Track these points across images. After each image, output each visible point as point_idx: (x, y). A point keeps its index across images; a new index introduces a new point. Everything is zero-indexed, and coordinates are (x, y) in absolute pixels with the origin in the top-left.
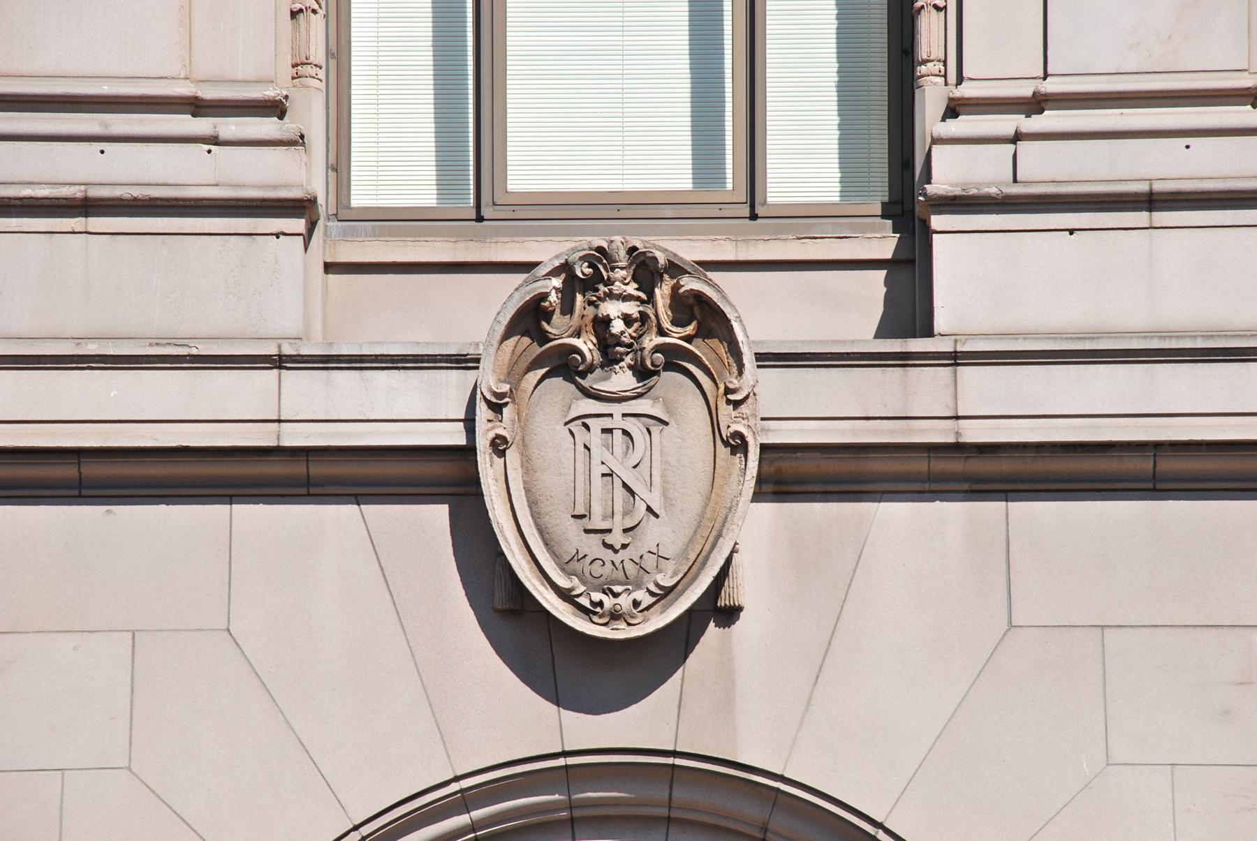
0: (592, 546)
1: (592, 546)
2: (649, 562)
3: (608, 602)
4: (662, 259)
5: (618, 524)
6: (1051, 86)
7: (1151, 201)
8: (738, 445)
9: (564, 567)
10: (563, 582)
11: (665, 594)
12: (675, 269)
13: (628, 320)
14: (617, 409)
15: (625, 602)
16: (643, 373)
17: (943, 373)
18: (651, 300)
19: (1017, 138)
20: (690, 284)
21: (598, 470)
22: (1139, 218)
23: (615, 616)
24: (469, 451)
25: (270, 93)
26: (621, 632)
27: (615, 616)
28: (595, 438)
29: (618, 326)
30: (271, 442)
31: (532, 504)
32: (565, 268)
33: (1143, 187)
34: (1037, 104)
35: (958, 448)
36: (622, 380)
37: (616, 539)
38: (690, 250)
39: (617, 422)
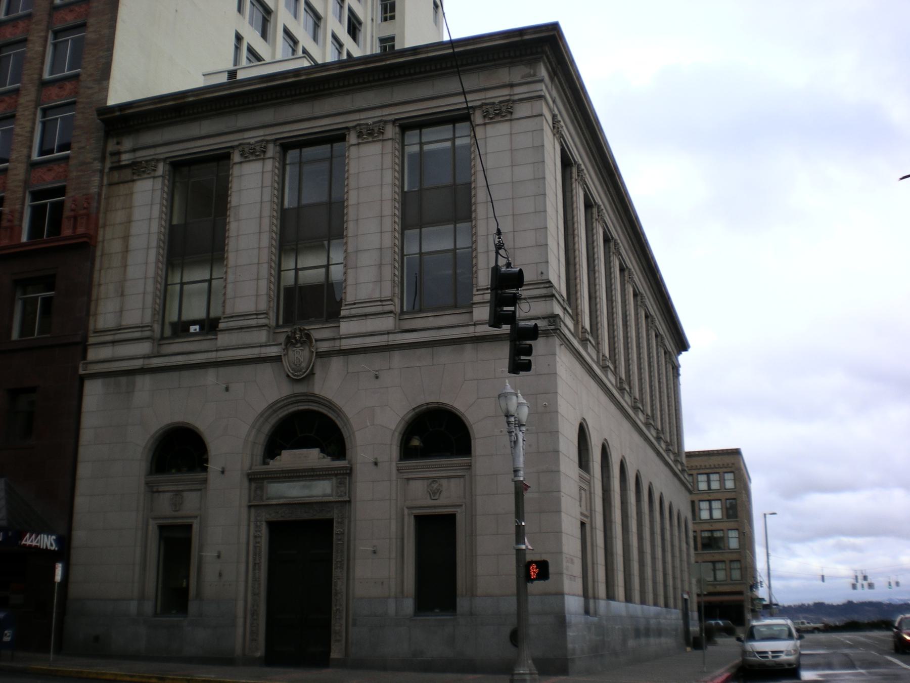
4: (302, 328)
8: (313, 352)
9: (292, 370)
10: (292, 372)
11: (305, 372)
12: (305, 329)
16: (301, 344)
17: (339, 340)
18: (301, 334)
20: (306, 332)
22: (364, 318)
25: (264, 312)
26: (298, 378)
27: (298, 376)
29: (298, 338)
30: (259, 357)
32: (291, 331)
36: (299, 345)
38: (307, 328)
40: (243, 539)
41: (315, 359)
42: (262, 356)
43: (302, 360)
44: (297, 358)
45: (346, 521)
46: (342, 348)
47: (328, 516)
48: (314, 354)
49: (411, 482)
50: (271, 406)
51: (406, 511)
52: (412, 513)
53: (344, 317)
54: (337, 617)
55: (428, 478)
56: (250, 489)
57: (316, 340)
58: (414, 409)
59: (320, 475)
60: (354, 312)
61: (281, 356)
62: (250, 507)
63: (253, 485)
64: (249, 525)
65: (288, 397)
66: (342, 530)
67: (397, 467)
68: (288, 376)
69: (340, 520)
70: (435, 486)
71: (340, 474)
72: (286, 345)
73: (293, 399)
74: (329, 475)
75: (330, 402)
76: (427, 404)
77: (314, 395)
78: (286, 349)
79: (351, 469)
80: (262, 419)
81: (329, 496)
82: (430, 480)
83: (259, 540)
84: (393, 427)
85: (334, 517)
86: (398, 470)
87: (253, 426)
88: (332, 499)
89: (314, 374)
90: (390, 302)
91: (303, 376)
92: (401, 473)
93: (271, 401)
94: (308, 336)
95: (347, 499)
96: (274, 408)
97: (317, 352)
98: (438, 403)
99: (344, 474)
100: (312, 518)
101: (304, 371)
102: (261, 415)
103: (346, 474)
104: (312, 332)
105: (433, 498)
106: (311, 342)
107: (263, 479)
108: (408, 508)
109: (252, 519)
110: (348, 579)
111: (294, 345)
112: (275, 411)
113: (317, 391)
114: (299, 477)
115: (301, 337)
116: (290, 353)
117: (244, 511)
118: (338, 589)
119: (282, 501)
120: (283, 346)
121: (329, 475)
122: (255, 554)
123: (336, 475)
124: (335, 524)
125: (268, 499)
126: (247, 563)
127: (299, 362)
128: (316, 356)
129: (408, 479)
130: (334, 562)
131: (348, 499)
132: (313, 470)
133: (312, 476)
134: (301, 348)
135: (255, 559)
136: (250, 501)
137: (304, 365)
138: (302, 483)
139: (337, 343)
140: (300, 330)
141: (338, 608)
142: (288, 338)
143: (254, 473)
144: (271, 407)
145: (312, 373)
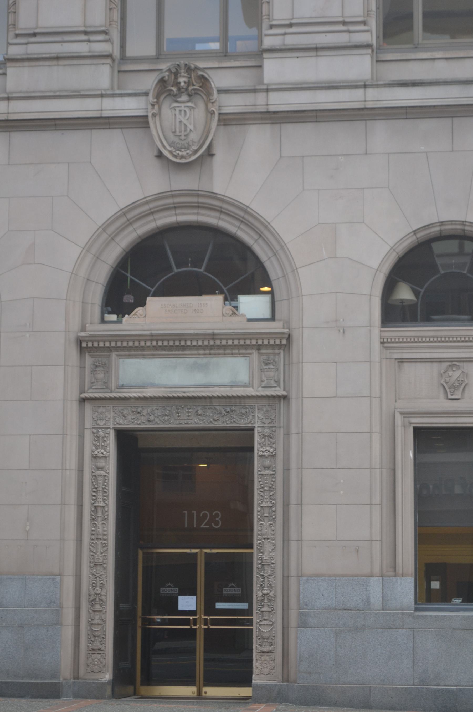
0: (176, 140)
1: (176, 140)
2: (191, 143)
3: (180, 153)
4: (193, 66)
5: (183, 133)
6: (294, 21)
7: (317, 49)
8: (213, 113)
9: (170, 146)
11: (196, 151)
12: (197, 68)
13: (185, 82)
14: (183, 105)
15: (184, 153)
16: (190, 96)
18: (190, 78)
19: (285, 34)
20: (200, 73)
21: (178, 120)
23: (182, 157)
24: (147, 117)
25: (103, 29)
26: (183, 161)
27: (182, 157)
28: (177, 112)
29: (182, 84)
31: (162, 130)
32: (169, 70)
33: (314, 46)
34: (291, 25)
35: (268, 112)
36: (184, 98)
37: (183, 137)
38: (201, 65)
39: (183, 108)
40: (72, 463)
41: (216, 130)
42: (106, 114)
43: (191, 127)
44: (180, 122)
45: (281, 434)
46: (272, 109)
47: (243, 423)
48: (216, 117)
49: (406, 365)
50: (124, 212)
51: (399, 419)
52: (411, 424)
53: (271, 50)
54: (266, 609)
55: (440, 361)
56: (82, 367)
57: (220, 91)
58: (415, 232)
59: (225, 347)
60: (291, 41)
61: (147, 117)
62: (83, 401)
63: (89, 360)
64: (81, 436)
65: (159, 197)
66: (271, 450)
67: (381, 337)
68: (160, 155)
69: (267, 431)
70: (455, 375)
71: (269, 346)
72: (158, 97)
73: (170, 201)
74: (246, 347)
75: (245, 210)
76: (442, 223)
77: (213, 196)
78: (157, 103)
79: (289, 338)
80: (105, 236)
82: (445, 365)
83: (101, 463)
84: (375, 264)
85: (256, 425)
86: (382, 343)
87: (87, 248)
88: (250, 391)
89: (212, 155)
90: (362, 27)
91: (193, 158)
92: (387, 348)
93: (124, 202)
94: (204, 81)
95: (280, 392)
96: (130, 216)
97: (220, 114)
98: (463, 223)
99: (274, 346)
101: (195, 148)
102: (105, 227)
103: (280, 346)
104: (209, 72)
105: (450, 397)
106: (209, 94)
107: (110, 349)
108: (402, 413)
109: (88, 424)
110: (286, 540)
111: (175, 97)
112: (130, 223)
113: (218, 188)
114: (184, 348)
115: (189, 83)
116: (166, 111)
117: (74, 407)
118: (265, 556)
119: (149, 393)
120: (151, 98)
122: (95, 490)
123: (259, 348)
124: (257, 438)
125: (122, 387)
126: (80, 506)
127: (185, 130)
128: (219, 120)
129: (401, 361)
130: (256, 508)
131: (285, 393)
132: (213, 336)
133: (211, 347)
134: (190, 104)
135: (94, 498)
136: (82, 392)
137: (194, 137)
138: (190, 361)
139: (261, 99)
140: (189, 69)
141: (265, 592)
142: (162, 81)
143: (93, 338)
144: (124, 214)
145: (210, 154)
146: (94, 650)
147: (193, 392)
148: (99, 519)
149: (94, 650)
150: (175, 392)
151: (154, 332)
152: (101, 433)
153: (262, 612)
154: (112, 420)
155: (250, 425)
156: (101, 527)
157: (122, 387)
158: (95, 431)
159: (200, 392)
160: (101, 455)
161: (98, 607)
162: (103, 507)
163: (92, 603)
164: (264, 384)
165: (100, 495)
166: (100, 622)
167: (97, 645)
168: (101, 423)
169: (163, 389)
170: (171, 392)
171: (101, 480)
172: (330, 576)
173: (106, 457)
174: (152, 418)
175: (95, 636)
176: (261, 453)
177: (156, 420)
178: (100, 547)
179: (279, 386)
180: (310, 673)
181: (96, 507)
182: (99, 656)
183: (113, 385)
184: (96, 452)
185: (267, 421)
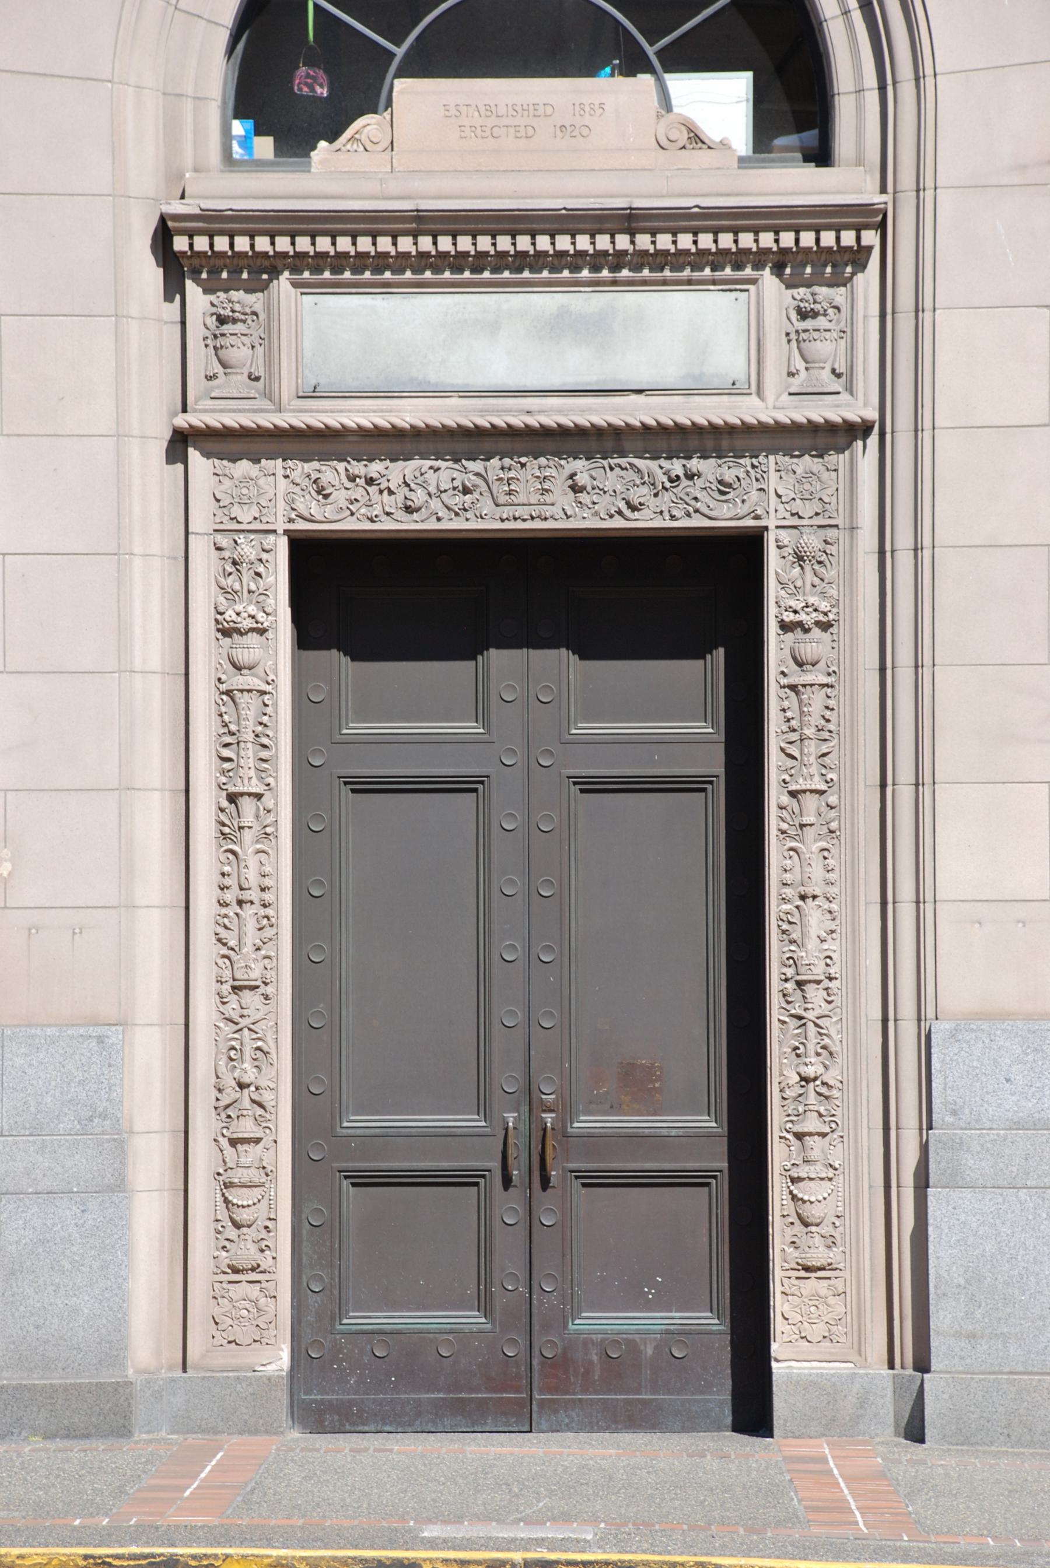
66: (824, 606)
74: (739, 259)
81: (733, 390)
83: (249, 649)
85: (771, 522)
100: (618, 523)
121: (739, 259)
124: (774, 562)
141: (810, 1071)
146: (236, 1271)
147: (560, 411)
148: (248, 836)
149: (236, 1271)
150: (498, 412)
151: (424, 205)
152: (248, 549)
153: (799, 1136)
154: (281, 505)
155: (750, 522)
156: (252, 861)
157: (314, 394)
158: (224, 541)
159: (583, 411)
160: (248, 624)
161: (247, 1128)
162: (259, 796)
163: (224, 1111)
164: (796, 385)
165: (249, 753)
166: (256, 1176)
167: (246, 1252)
168: (246, 515)
169: (455, 401)
170: (483, 412)
171: (249, 705)
172: (1029, 1017)
173: (262, 632)
174: (419, 497)
175: (237, 1225)
176: (789, 617)
177: (435, 504)
178: (251, 926)
179: (850, 389)
180: (972, 1336)
181: (232, 798)
182: (254, 1291)
183: (287, 388)
184: (230, 615)
185: (807, 509)
